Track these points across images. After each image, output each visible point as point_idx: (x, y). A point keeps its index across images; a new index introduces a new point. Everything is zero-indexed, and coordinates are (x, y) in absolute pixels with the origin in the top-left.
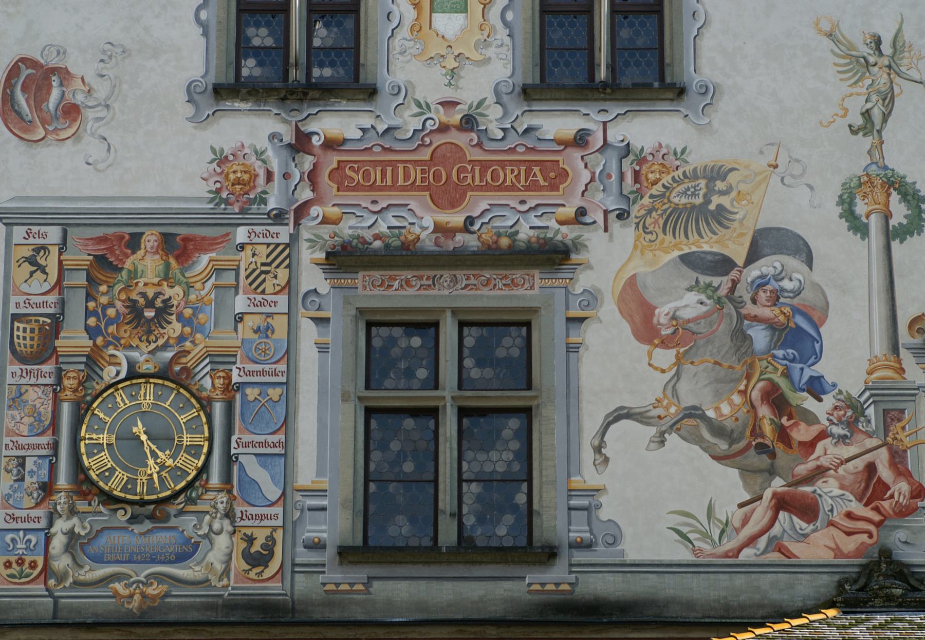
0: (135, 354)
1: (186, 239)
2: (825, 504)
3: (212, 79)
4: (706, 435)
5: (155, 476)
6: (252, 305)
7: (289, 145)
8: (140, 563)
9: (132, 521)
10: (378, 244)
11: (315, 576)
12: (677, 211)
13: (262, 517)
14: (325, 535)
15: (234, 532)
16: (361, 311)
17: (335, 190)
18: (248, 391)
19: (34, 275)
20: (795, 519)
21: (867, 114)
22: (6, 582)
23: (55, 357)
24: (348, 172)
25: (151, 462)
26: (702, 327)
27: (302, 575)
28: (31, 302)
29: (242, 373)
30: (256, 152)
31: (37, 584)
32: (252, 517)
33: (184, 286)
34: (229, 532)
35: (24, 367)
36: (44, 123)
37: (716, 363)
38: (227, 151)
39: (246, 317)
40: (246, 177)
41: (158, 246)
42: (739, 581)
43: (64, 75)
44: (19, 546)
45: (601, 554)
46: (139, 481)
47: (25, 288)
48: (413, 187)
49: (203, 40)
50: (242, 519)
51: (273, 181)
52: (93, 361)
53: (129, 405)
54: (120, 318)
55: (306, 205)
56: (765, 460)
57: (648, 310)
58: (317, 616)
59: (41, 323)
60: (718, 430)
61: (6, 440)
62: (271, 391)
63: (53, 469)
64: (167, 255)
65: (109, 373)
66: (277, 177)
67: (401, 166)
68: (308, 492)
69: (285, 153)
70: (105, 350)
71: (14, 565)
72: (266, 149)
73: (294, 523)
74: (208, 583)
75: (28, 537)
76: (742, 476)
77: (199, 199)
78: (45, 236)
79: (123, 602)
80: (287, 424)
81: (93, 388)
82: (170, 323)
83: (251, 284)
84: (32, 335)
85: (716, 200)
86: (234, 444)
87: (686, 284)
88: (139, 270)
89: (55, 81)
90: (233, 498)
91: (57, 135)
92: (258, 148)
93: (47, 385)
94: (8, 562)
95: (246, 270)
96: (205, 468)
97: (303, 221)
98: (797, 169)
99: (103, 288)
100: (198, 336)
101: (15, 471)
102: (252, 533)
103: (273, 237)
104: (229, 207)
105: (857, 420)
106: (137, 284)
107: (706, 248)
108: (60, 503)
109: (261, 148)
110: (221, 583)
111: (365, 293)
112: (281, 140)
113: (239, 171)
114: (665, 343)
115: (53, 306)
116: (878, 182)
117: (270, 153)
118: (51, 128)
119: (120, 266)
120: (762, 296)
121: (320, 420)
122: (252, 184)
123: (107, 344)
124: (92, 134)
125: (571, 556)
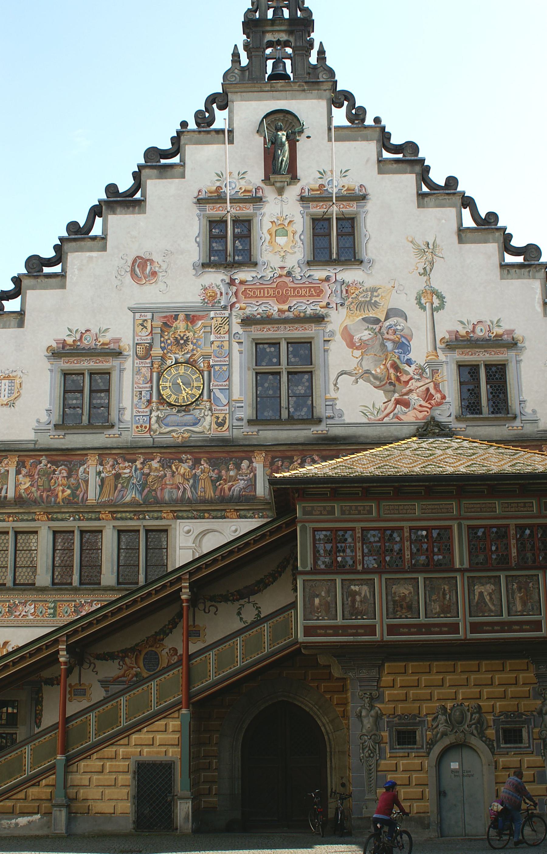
0: (177, 356)
1: (194, 316)
2: (412, 402)
3: (201, 261)
4: (372, 379)
5: (185, 397)
10: (259, 316)
13: (222, 410)
14: (243, 416)
16: (254, 339)
18: (216, 367)
20: (403, 407)
21: (425, 269)
25: (184, 392)
32: (218, 410)
37: (375, 355)
38: (207, 286)
39: (214, 342)
40: (213, 294)
42: (384, 428)
43: (152, 261)
45: (337, 421)
47: (140, 334)
48: (270, 296)
49: (198, 248)
55: (234, 303)
57: (352, 337)
58: (241, 443)
60: (376, 378)
61: (135, 386)
62: (223, 367)
63: (151, 395)
65: (169, 362)
66: (224, 294)
67: (266, 289)
69: (227, 286)
73: (233, 412)
76: (384, 393)
77: (198, 302)
78: (146, 316)
80: (229, 378)
85: (374, 299)
86: (211, 386)
87: (364, 328)
89: (148, 263)
96: (202, 394)
97: (233, 309)
98: (401, 288)
99: (166, 333)
100: (198, 349)
105: (423, 373)
107: (371, 315)
111: (256, 333)
114: (357, 348)
116: (429, 292)
117: (221, 286)
120: (390, 331)
123: (168, 352)
125: (326, 421)
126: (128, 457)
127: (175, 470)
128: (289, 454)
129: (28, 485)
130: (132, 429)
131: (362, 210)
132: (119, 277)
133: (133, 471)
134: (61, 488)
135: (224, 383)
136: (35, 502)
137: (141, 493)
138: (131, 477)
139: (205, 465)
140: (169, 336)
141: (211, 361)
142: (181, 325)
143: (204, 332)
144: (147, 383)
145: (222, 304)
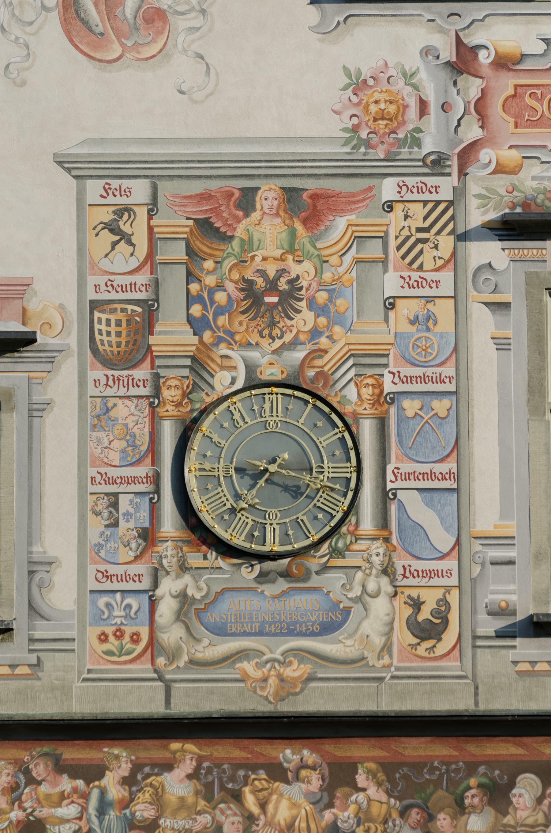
0: (254, 355)
1: (315, 197)
6: (406, 286)
7: (448, 64)
8: (275, 635)
9: (262, 579)
11: (503, 652)
13: (430, 574)
15: (396, 594)
17: (512, 125)
19: (117, 247)
22: (102, 661)
23: (149, 358)
24: (527, 99)
27: (487, 650)
28: (115, 284)
29: (397, 380)
30: (404, 74)
31: (142, 663)
32: (418, 574)
33: (316, 260)
34: (388, 594)
35: (110, 373)
36: (119, 35)
38: (366, 73)
39: (399, 303)
40: (392, 109)
41: (278, 207)
44: (116, 613)
46: (268, 527)
47: (105, 264)
50: (404, 576)
51: (429, 114)
52: (200, 364)
53: (250, 423)
54: (232, 305)
59: (129, 312)
64: (291, 218)
69: (444, 75)
70: (214, 349)
71: (111, 638)
72: (418, 69)
73: (473, 581)
74: (364, 662)
75: (126, 601)
77: (331, 140)
78: (128, 193)
79: (255, 687)
81: (203, 401)
82: (298, 311)
83: (403, 257)
84: (119, 329)
86: (390, 476)
88: (255, 238)
90: (391, 549)
91: (138, 52)
92: (407, 68)
93: (142, 397)
94: (103, 634)
95: (397, 237)
97: (470, 170)
99: (209, 264)
100: (337, 329)
101: (105, 514)
102: (419, 596)
103: (431, 192)
104: (371, 151)
106: (253, 258)
108: (166, 556)
109: (411, 68)
110: (381, 662)
112: (438, 57)
113: (382, 100)
115: (143, 289)
117: (423, 75)
118: (129, 43)
119: (229, 234)
121: (501, 442)
122: (400, 118)
123: (218, 341)
124: (185, 51)
127: (255, 810)
130: (82, 645)
132: (16, 31)
133: (92, 810)
135: (439, 468)
141: (387, 379)
143: (358, 261)
144: (138, 462)
145: (425, 151)
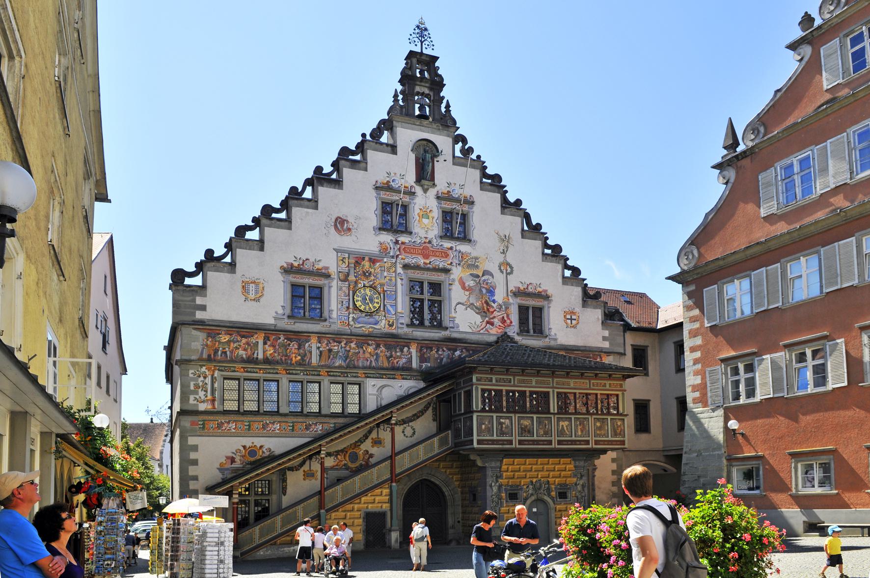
1: (374, 260)
2: (495, 323)
3: (378, 226)
12: (469, 265)
21: (503, 250)
26: (474, 288)
42: (480, 336)
43: (348, 222)
48: (419, 254)
56: (484, 314)
60: (477, 308)
63: (349, 304)
68: (400, 313)
80: (396, 299)
85: (476, 263)
98: (491, 259)
114: (467, 290)
126: (336, 339)
128: (430, 345)
129: (272, 351)
131: (471, 210)
134: (294, 355)
136: (278, 363)
137: (345, 361)
138: (338, 352)
139: (382, 348)
140: (359, 270)
142: (366, 264)
